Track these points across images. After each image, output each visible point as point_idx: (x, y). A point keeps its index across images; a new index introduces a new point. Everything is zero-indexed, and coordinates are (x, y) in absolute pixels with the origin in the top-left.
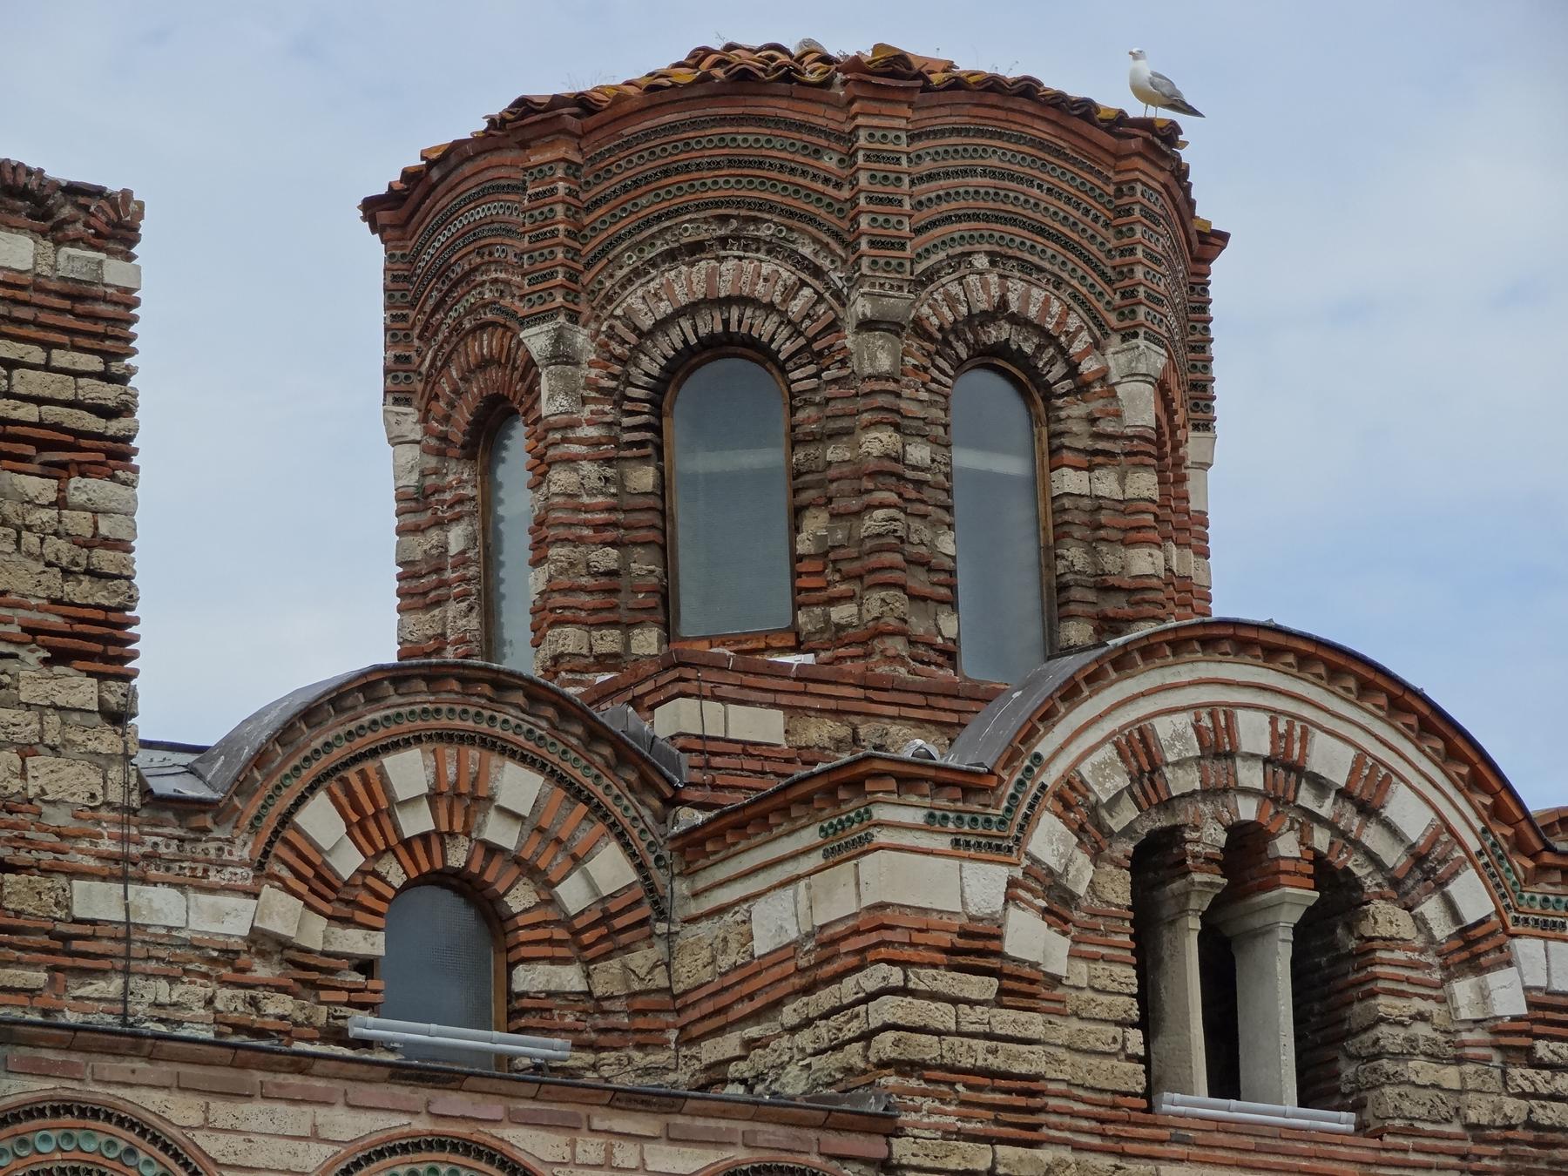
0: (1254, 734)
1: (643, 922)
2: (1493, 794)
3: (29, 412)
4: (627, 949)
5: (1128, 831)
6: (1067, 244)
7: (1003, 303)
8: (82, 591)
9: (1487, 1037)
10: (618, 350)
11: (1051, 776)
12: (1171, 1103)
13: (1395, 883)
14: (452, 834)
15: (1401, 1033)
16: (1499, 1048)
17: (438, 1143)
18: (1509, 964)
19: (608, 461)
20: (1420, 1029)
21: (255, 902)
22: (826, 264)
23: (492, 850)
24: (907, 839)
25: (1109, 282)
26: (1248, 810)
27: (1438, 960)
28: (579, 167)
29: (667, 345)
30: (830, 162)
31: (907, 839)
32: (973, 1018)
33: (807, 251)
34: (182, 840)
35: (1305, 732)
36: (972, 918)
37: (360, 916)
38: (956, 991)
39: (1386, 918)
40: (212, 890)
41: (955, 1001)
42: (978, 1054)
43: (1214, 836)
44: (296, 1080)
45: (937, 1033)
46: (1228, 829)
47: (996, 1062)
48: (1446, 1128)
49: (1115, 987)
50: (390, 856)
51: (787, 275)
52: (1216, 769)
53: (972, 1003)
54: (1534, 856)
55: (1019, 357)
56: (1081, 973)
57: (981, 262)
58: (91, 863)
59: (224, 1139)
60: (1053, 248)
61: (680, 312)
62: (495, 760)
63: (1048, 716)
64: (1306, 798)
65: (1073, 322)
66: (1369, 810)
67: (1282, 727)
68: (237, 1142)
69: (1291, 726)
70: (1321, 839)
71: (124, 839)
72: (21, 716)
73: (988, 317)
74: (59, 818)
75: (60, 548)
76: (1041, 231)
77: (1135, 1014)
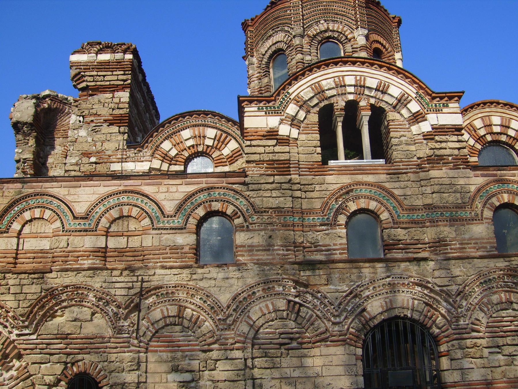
0: (350, 80)
1: (241, 154)
2: (418, 84)
3: (108, 83)
4: (237, 160)
5: (317, 104)
6: (343, 15)
7: (328, 28)
8: (117, 112)
9: (422, 137)
10: (260, 59)
11: (292, 97)
12: (332, 163)
13: (394, 107)
14: (200, 145)
15: (397, 139)
16: (425, 139)
17: (125, 192)
18: (426, 120)
19: (260, 79)
20: (403, 139)
21: (150, 163)
22: (289, 30)
23: (208, 146)
24: (253, 114)
25: (353, 20)
26: (351, 97)
27: (407, 123)
28: (253, 31)
29: (267, 55)
30: (288, 12)
31: (253, 114)
32: (268, 149)
33: (286, 29)
34: (135, 153)
35: (365, 79)
36: (270, 128)
37: (178, 163)
38: (264, 144)
39: (392, 115)
40: (143, 161)
41: (264, 146)
42: (271, 157)
43: (342, 104)
44: (92, 182)
45: (260, 154)
46: (346, 102)
47: (274, 158)
48: (412, 160)
49: (313, 139)
50: (185, 151)
51: (283, 35)
52: (340, 91)
53: (269, 146)
54: (430, 95)
55: (334, 38)
56: (303, 137)
57: (322, 22)
58: (115, 160)
59: (72, 196)
60: (339, 17)
61: (268, 49)
62: (206, 128)
63: (290, 84)
64: (367, 92)
65: (345, 29)
66: (384, 92)
67: (358, 78)
68: (76, 197)
69: (361, 78)
70: (372, 101)
71: (122, 155)
72: (102, 136)
73: (325, 31)
74: (109, 153)
75: (112, 105)
76: (337, 14)
77: (319, 144)
